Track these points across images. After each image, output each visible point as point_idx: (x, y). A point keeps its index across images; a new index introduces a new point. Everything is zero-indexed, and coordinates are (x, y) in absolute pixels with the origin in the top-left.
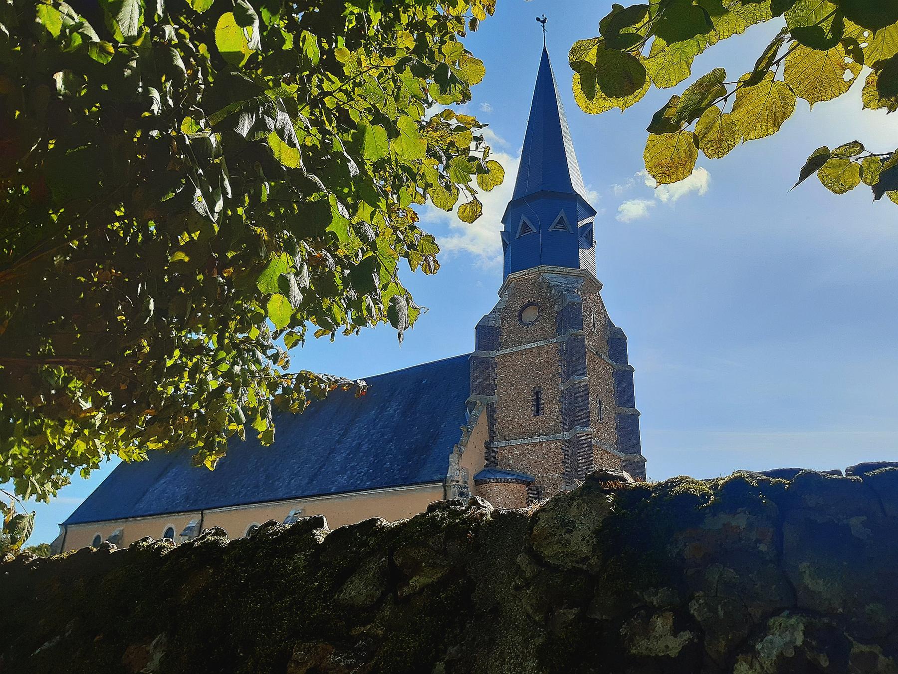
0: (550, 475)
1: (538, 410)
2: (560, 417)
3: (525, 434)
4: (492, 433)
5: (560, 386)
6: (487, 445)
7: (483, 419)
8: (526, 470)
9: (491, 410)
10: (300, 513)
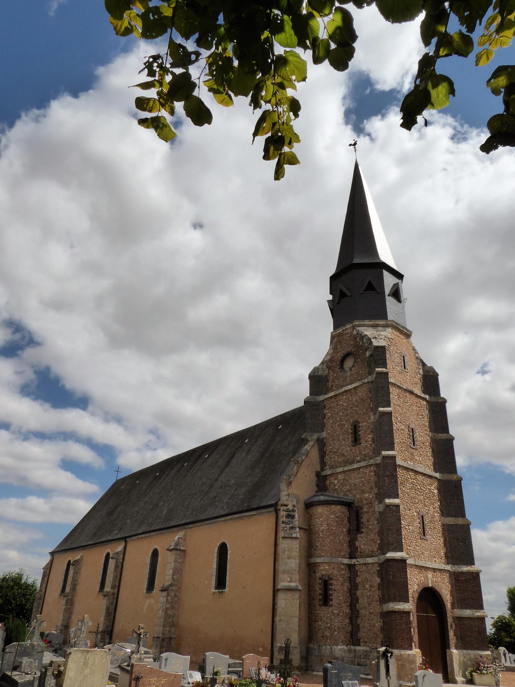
0: (366, 495)
1: (356, 440)
2: (373, 445)
3: (347, 462)
4: (323, 464)
5: (372, 417)
6: (318, 474)
7: (315, 454)
8: (348, 493)
9: (321, 443)
10: (182, 537)
